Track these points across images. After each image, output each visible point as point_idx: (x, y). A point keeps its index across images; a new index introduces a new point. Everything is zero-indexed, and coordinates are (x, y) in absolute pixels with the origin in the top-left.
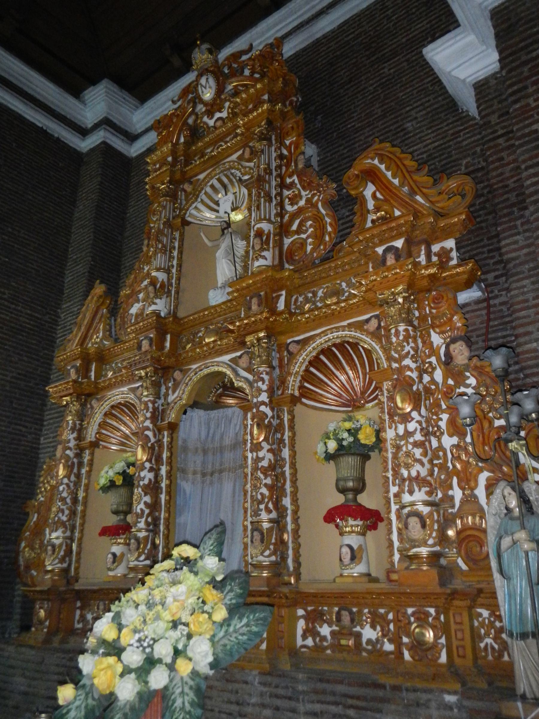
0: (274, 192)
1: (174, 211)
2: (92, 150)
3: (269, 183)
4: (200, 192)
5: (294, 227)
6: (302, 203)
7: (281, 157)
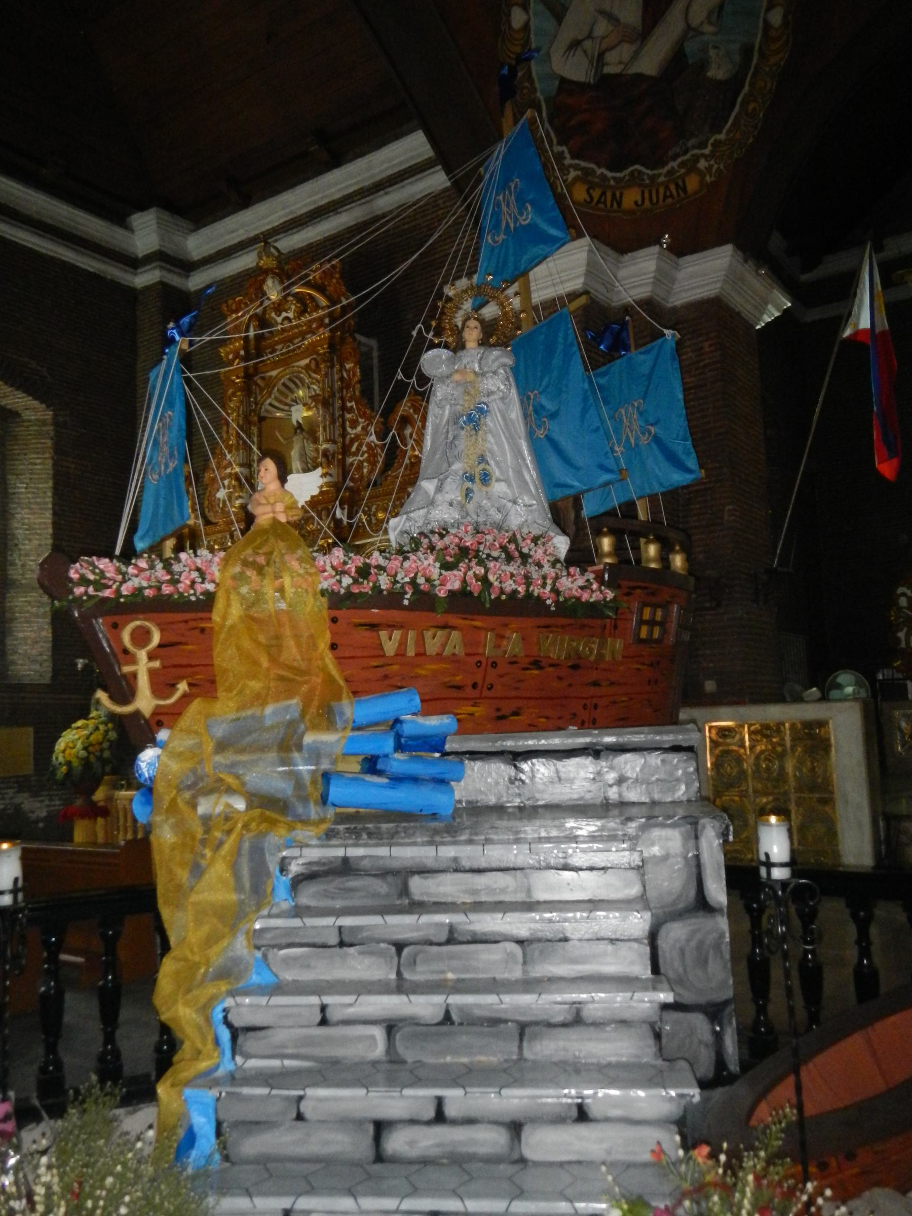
0: (337, 414)
1: (250, 406)
2: (147, 288)
3: (333, 405)
4: (273, 389)
6: (359, 429)
7: (342, 379)
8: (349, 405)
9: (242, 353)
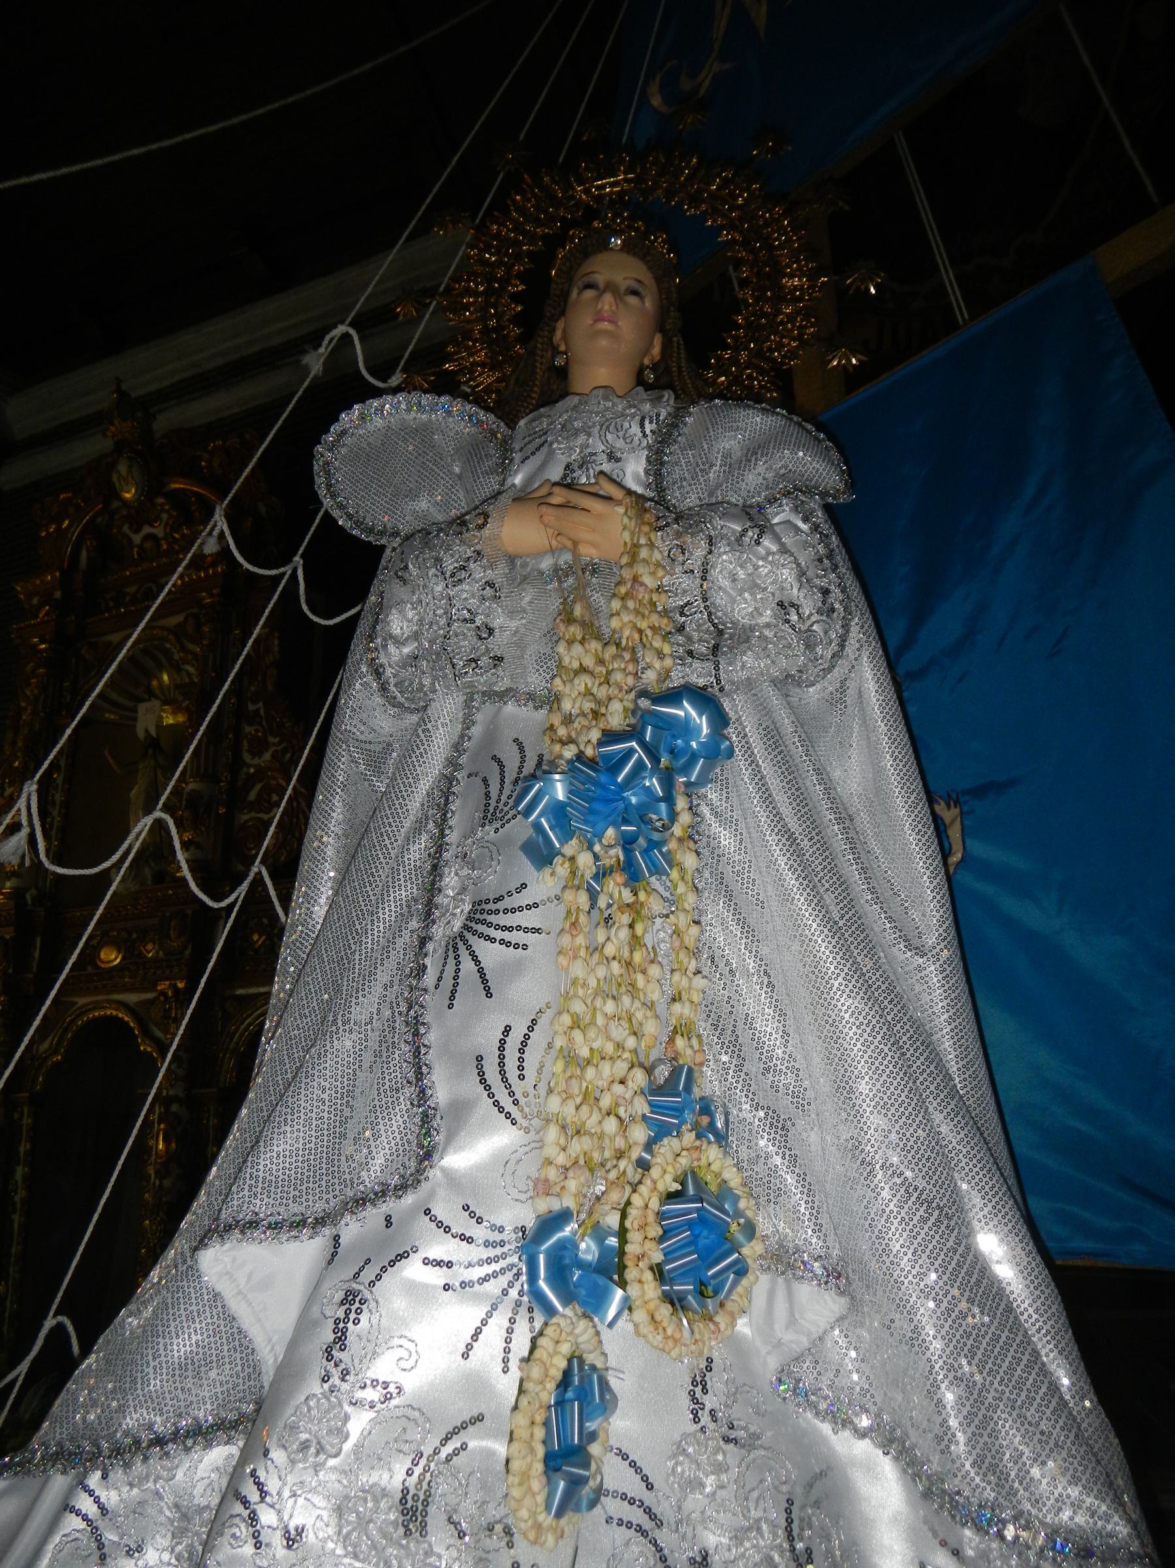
5: (252, 796)
6: (267, 756)
8: (251, 707)
9: (58, 594)
